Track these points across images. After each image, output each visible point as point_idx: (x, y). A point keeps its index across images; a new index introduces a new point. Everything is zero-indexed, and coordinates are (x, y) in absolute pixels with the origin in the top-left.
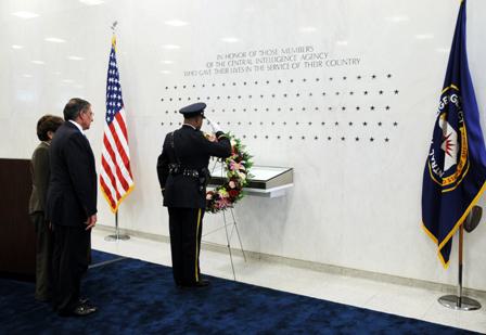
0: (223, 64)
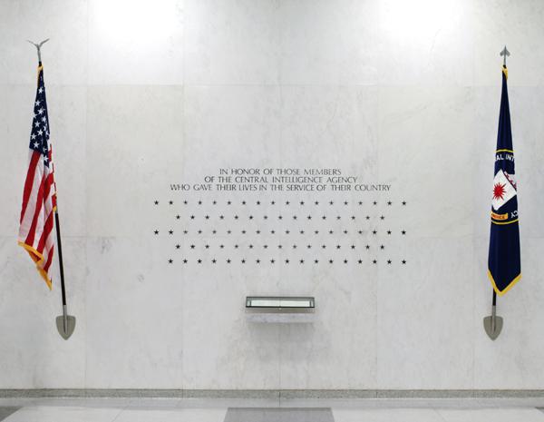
0: (228, 180)
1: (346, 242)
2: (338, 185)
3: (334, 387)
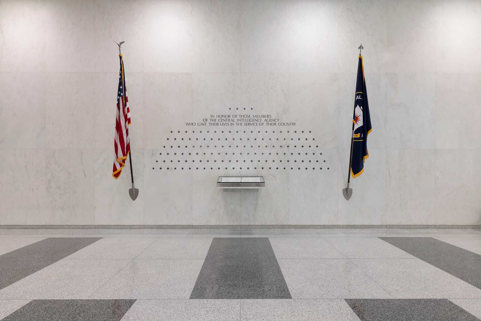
0: (215, 120)
1: (274, 151)
2: (270, 123)
3: (268, 224)
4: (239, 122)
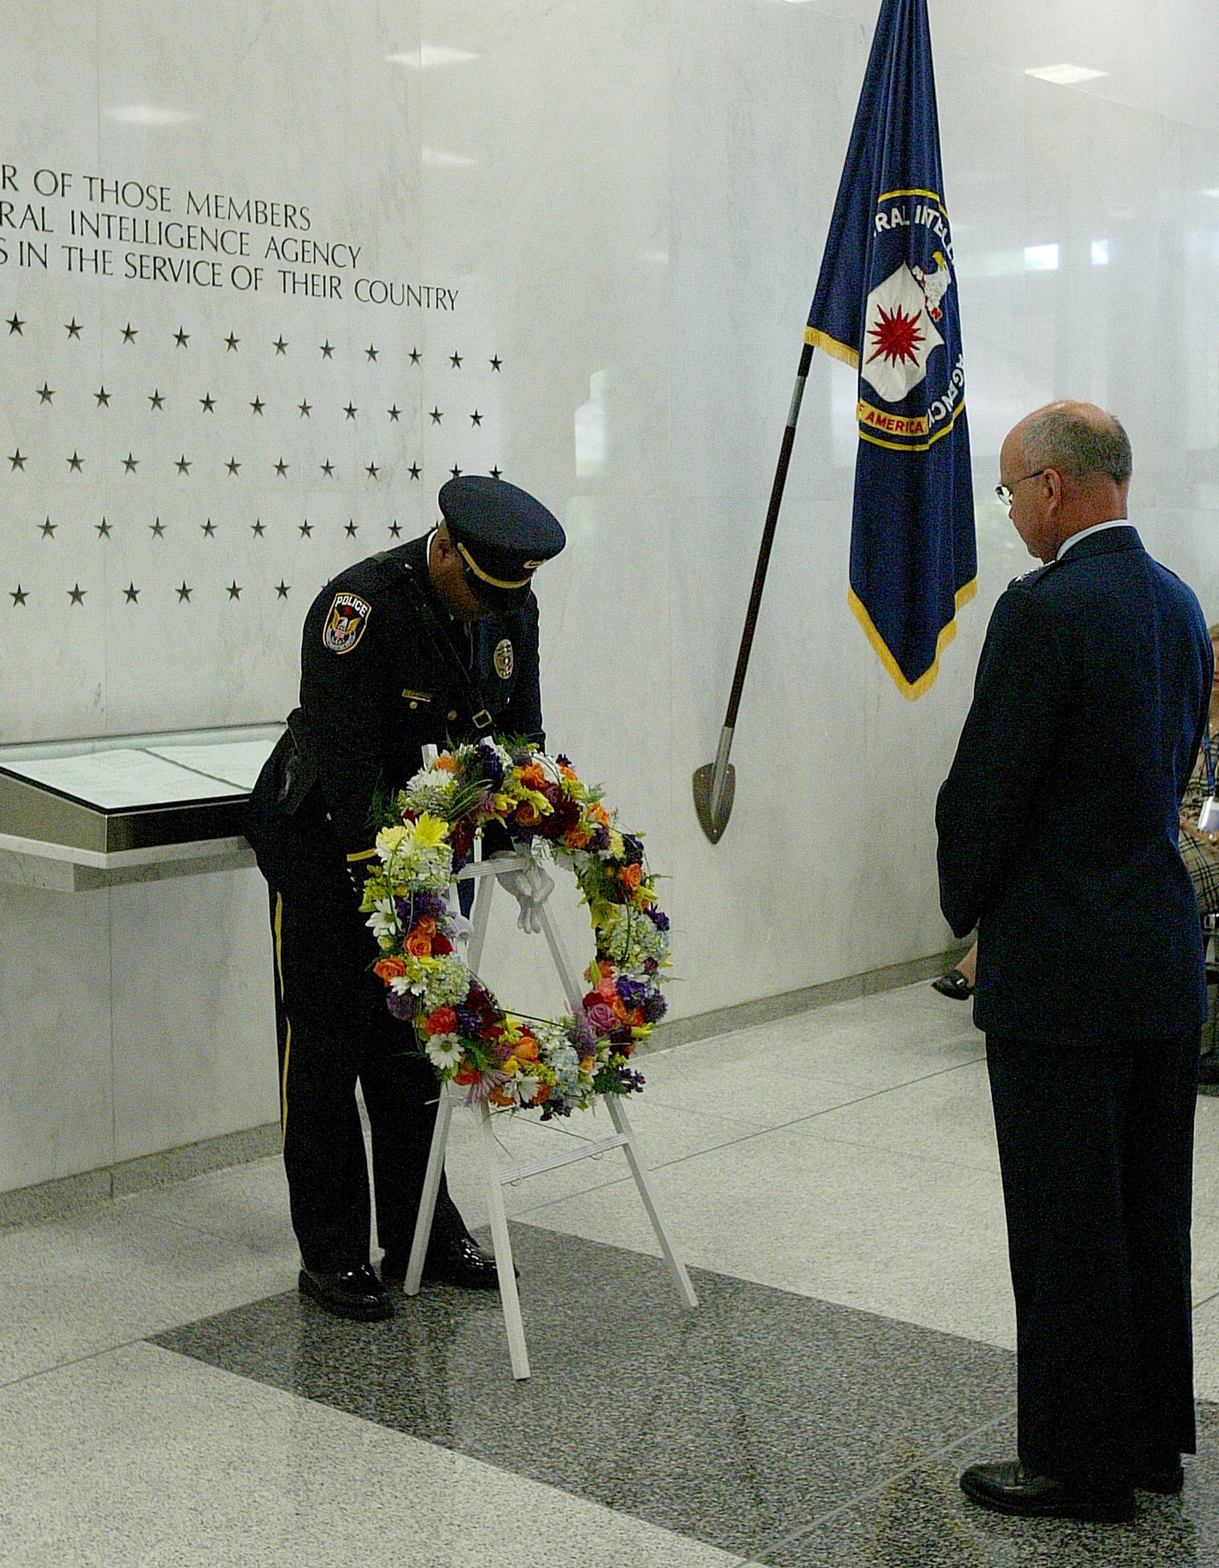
4: (89, 243)
